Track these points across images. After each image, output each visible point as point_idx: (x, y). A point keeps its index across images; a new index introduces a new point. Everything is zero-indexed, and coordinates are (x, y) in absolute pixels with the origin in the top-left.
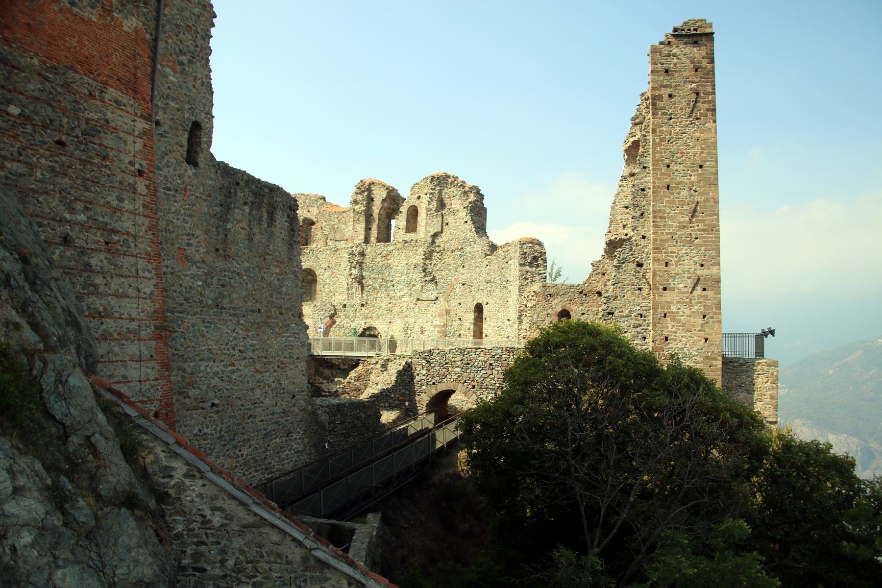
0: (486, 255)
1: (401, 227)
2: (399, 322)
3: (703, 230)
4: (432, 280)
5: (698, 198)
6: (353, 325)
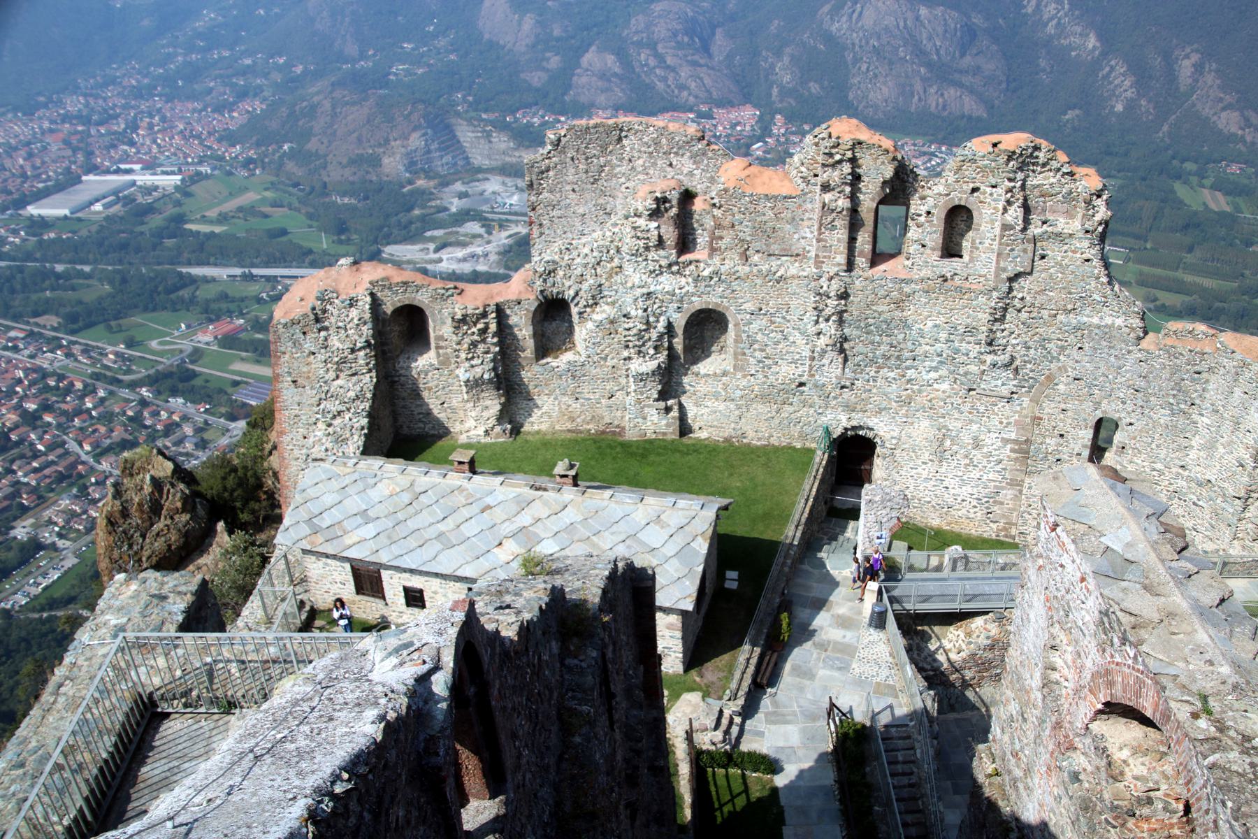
0: (1139, 339)
1: (929, 244)
2: (925, 423)
4: (1006, 366)
6: (824, 420)
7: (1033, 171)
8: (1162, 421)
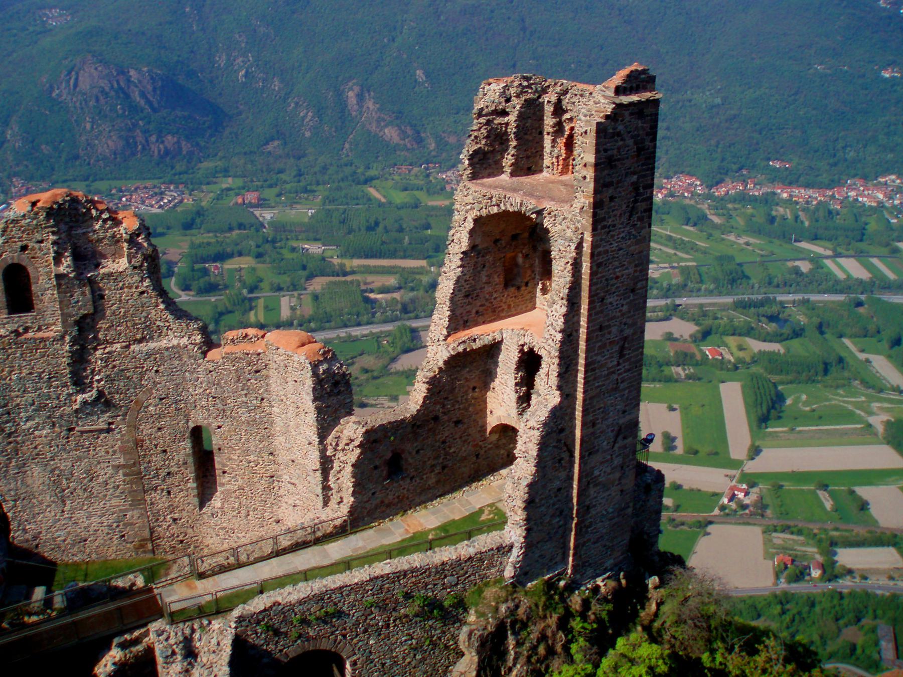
3: (629, 370)
5: (628, 332)
7: (77, 221)
8: (243, 419)
